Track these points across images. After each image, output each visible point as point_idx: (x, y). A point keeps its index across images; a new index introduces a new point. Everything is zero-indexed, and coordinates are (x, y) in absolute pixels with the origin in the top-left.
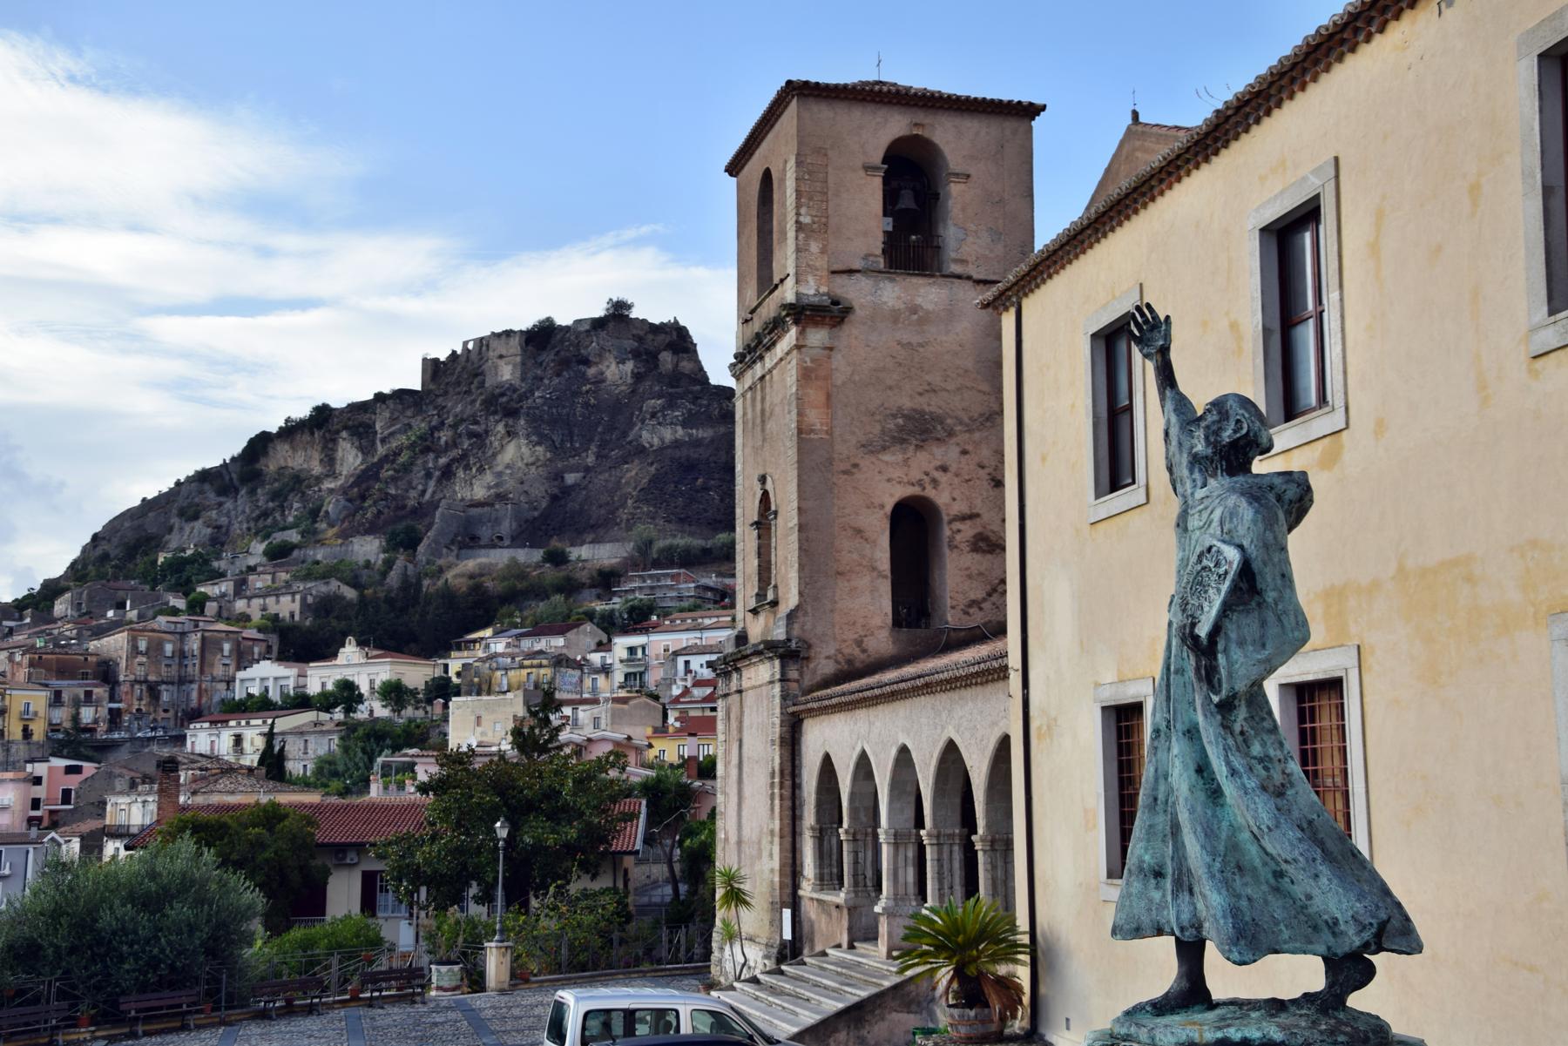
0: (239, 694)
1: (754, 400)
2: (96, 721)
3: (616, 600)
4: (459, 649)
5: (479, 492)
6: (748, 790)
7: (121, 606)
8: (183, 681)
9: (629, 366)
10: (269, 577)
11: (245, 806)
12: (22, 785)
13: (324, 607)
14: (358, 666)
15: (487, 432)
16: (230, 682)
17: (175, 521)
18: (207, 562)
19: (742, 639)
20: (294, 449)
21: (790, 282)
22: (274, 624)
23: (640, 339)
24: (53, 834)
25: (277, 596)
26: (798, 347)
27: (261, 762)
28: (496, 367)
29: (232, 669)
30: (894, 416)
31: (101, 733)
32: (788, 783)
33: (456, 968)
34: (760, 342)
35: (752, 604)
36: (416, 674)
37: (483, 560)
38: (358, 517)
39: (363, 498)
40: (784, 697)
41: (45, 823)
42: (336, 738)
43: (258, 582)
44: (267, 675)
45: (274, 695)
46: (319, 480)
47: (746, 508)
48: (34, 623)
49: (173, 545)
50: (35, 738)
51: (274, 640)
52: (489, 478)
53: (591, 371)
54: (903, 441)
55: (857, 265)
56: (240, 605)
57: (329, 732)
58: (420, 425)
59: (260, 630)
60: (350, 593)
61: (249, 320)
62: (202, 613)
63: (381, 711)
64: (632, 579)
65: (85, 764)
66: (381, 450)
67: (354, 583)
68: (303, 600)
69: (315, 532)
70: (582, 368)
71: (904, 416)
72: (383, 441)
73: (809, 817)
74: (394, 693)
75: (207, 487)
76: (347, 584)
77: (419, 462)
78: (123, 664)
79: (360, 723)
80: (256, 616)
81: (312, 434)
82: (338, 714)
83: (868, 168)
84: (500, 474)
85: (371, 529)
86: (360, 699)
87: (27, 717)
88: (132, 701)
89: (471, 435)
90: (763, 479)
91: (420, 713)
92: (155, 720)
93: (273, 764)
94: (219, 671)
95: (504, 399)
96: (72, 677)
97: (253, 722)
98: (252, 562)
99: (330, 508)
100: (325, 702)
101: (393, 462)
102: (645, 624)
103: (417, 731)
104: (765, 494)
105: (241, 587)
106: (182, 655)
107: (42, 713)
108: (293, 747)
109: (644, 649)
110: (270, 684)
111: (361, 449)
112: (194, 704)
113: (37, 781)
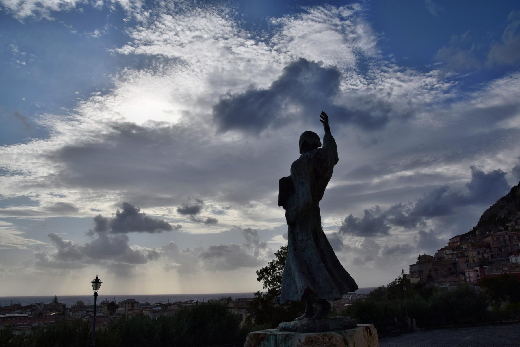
7: (490, 231)
31: (490, 260)
56: (517, 227)
87: (473, 257)
113: (477, 271)
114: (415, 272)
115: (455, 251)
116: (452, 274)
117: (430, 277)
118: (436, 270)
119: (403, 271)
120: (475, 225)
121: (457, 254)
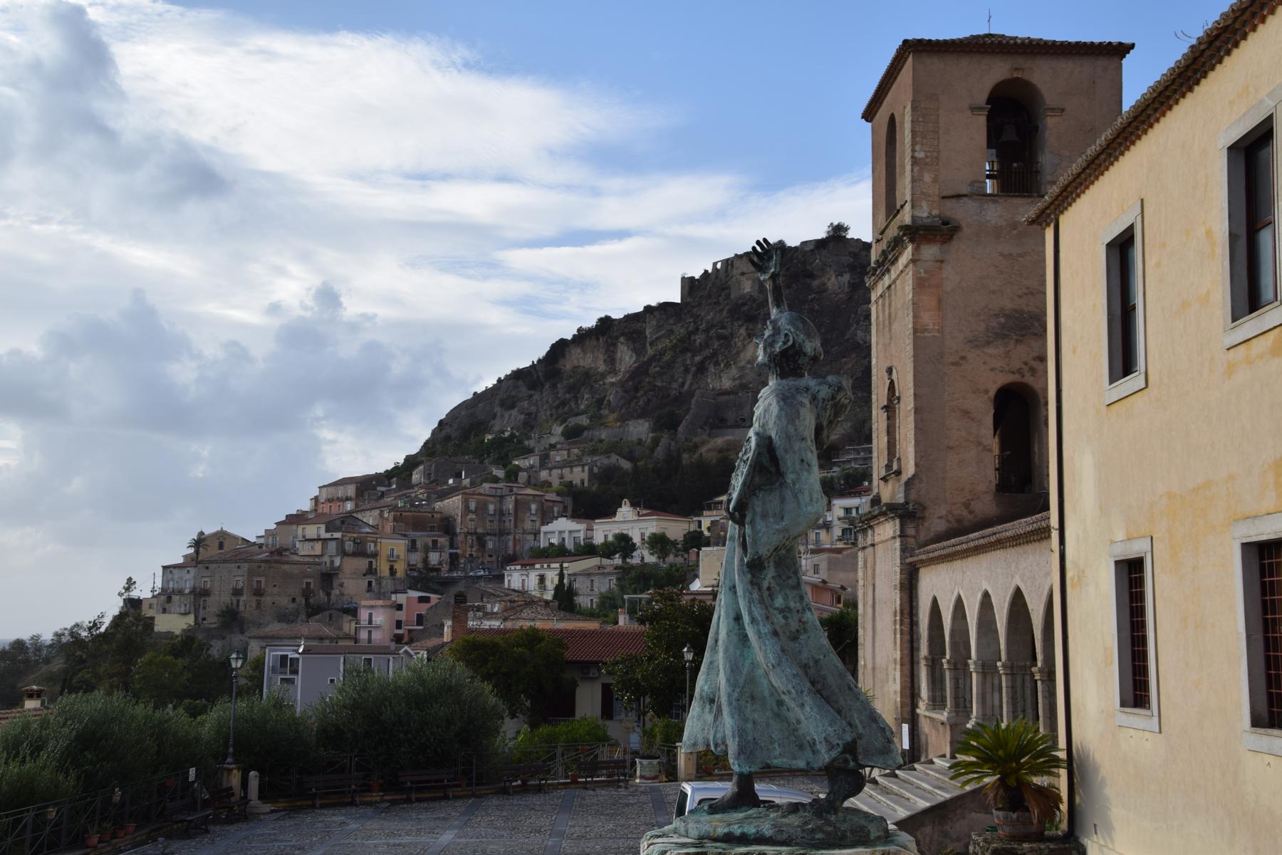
0: (543, 544)
1: (883, 305)
2: (440, 563)
3: (836, 469)
4: (710, 509)
5: (727, 383)
6: (879, 626)
7: (458, 475)
8: (502, 533)
9: (846, 277)
10: (565, 453)
11: (513, 631)
12: (388, 610)
13: (606, 476)
14: (629, 521)
15: (732, 335)
16: (536, 534)
17: (498, 409)
18: (520, 442)
19: (876, 501)
20: (584, 352)
21: (908, 207)
22: (568, 489)
23: (855, 255)
24: (406, 648)
25: (571, 467)
26: (914, 261)
27: (555, 596)
28: (739, 283)
29: (538, 524)
30: (996, 316)
31: (445, 573)
32: (907, 621)
33: (655, 762)
34: (886, 258)
35: (883, 473)
36: (676, 529)
37: (730, 437)
38: (633, 404)
39: (636, 389)
40: (904, 550)
41: (406, 639)
42: (614, 578)
43: (558, 457)
44: (563, 529)
45: (569, 545)
46: (603, 376)
47: (879, 396)
48: (399, 488)
49: (496, 428)
51: (569, 501)
52: (734, 371)
53: (816, 283)
54: (1004, 337)
55: (965, 190)
56: (544, 474)
57: (609, 574)
58: (680, 331)
59: (558, 494)
60: (626, 465)
61: (579, 249)
62: (516, 481)
63: (651, 559)
64: (848, 452)
65: (432, 596)
66: (650, 351)
67: (630, 457)
68: (591, 470)
69: (601, 417)
70: (808, 280)
71: (1005, 316)
72: (652, 344)
73: (924, 650)
74: (659, 543)
75: (520, 383)
76: (624, 458)
77: (679, 360)
78: (459, 520)
79: (633, 567)
80: (556, 483)
81: (598, 339)
82: (617, 560)
83: (974, 109)
84: (742, 368)
85: (643, 415)
86: (633, 547)
87: (392, 559)
88: (466, 548)
89: (720, 337)
90: (890, 371)
91: (679, 560)
92: (483, 563)
93: (565, 598)
94: (528, 525)
95: (746, 308)
96: (424, 529)
97: (553, 565)
98: (553, 440)
99: (611, 398)
100: (607, 550)
101: (659, 360)
102: (858, 489)
103: (677, 574)
104: (892, 383)
105: (544, 459)
106: (501, 513)
107: (402, 557)
108: (581, 585)
109: (857, 509)
110: (566, 535)
111: (634, 350)
112: (511, 552)
113: (399, 607)
114: (181, 592)
115: (337, 530)
116: (313, 611)
117: (231, 619)
118: (258, 592)
119: (130, 583)
120: (414, 449)
121: (341, 542)
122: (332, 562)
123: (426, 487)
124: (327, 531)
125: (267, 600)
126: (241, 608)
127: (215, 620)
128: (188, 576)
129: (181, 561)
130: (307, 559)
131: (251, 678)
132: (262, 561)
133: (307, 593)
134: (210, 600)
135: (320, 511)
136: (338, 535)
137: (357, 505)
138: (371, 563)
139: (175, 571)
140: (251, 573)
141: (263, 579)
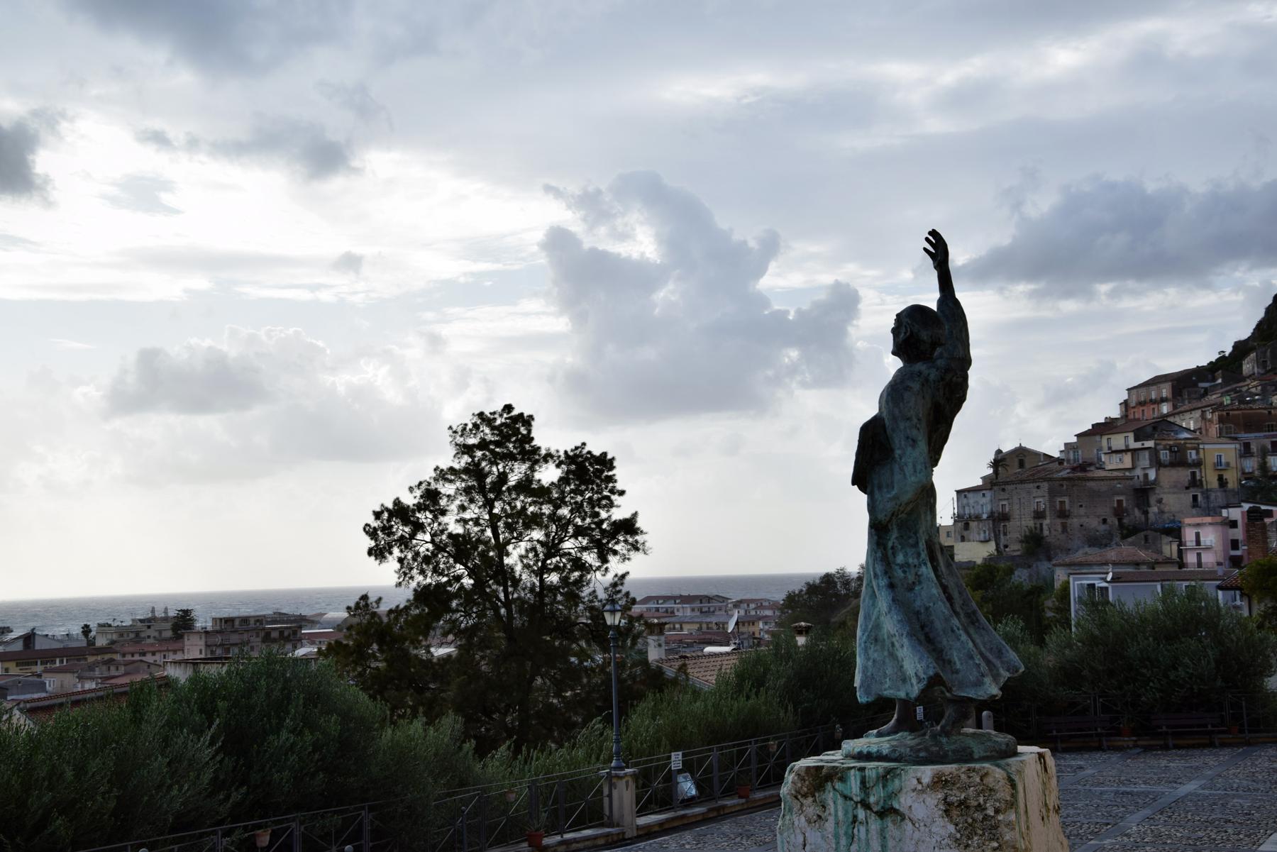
12: (1220, 528)
48: (1225, 383)
50: (1230, 486)
113: (1233, 524)
114: (978, 518)
115: (1147, 438)
116: (1128, 532)
117: (1036, 545)
118: (1063, 514)
121: (1154, 452)
122: (1146, 476)
123: (1260, 377)
124: (1136, 440)
125: (1074, 522)
126: (1046, 533)
127: (1017, 546)
128: (984, 500)
129: (980, 483)
130: (1115, 474)
131: (1058, 610)
132: (1064, 479)
133: (1119, 512)
134: (1011, 525)
135: (1131, 417)
136: (1150, 444)
137: (1175, 407)
138: (1193, 474)
139: (970, 495)
140: (1052, 493)
141: (1066, 499)
